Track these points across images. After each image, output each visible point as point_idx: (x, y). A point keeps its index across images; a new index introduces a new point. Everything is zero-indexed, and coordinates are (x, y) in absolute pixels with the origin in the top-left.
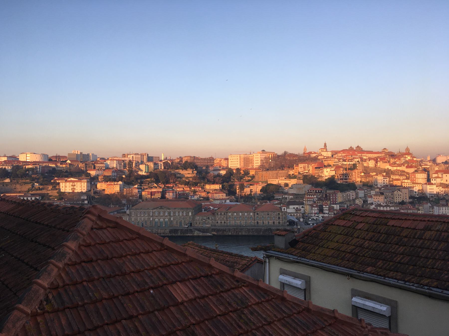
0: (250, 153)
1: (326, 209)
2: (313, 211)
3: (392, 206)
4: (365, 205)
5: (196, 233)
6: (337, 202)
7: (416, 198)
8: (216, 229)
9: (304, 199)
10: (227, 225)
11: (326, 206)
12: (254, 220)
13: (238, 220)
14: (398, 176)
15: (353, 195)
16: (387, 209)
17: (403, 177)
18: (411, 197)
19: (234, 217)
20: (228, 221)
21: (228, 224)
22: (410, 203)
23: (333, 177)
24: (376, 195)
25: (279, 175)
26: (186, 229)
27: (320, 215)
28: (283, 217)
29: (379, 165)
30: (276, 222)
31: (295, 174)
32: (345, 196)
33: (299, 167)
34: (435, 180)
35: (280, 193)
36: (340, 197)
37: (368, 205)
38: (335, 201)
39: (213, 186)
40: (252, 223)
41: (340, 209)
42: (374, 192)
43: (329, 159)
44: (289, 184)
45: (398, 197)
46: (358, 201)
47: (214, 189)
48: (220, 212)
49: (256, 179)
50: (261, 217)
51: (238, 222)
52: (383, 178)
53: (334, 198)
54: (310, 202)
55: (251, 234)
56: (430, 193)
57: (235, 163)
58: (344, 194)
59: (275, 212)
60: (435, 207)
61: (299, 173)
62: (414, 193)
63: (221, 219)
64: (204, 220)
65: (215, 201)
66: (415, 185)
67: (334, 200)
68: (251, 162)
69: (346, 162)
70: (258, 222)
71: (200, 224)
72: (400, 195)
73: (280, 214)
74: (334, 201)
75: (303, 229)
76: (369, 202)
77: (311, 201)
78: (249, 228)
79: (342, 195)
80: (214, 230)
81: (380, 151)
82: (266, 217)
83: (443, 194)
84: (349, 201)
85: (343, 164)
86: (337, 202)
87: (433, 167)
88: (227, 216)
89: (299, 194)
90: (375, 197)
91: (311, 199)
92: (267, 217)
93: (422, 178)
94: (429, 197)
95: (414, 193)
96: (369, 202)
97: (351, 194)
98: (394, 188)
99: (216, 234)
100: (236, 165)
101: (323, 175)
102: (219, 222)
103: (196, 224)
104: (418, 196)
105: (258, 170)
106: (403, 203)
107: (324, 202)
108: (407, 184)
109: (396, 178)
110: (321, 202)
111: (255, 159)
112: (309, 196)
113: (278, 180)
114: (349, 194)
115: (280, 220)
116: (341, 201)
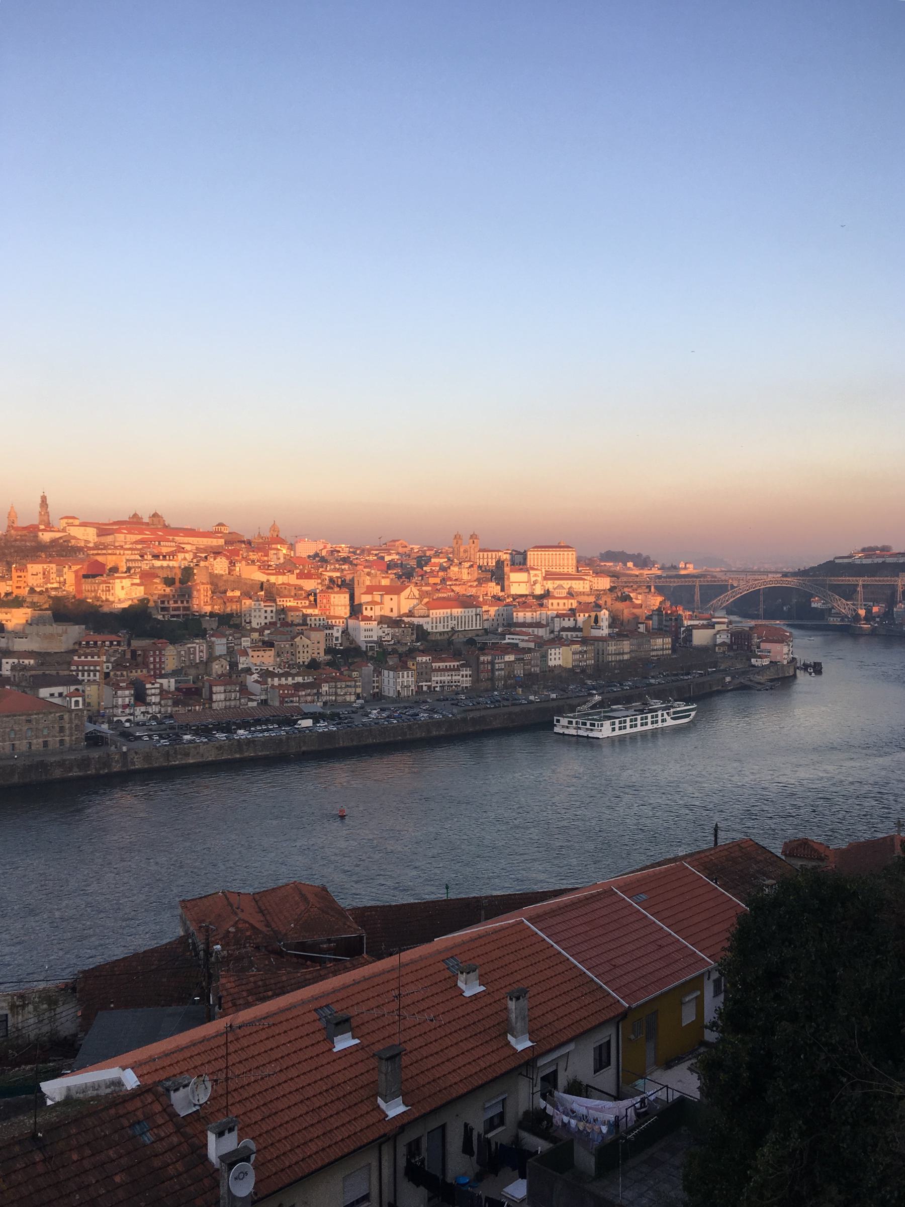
1: (153, 691)
2: (120, 701)
3: (298, 674)
4: (235, 675)
6: (163, 672)
7: (339, 651)
9: (73, 668)
11: (153, 684)
14: (292, 599)
16: (286, 682)
17: (303, 602)
18: (328, 651)
22: (330, 664)
23: (144, 602)
24: (255, 648)
27: (138, 708)
29: (238, 569)
30: (54, 742)
31: (16, 592)
32: (183, 653)
33: (30, 573)
36: (171, 657)
37: (242, 675)
38: (161, 669)
41: (176, 689)
42: (247, 641)
43: (110, 552)
45: (301, 652)
46: (217, 667)
50: (8, 730)
52: (265, 606)
53: (158, 660)
54: (92, 674)
56: (366, 639)
58: (180, 648)
59: (51, 713)
60: (386, 672)
61: (32, 591)
62: (334, 639)
66: (336, 622)
67: (158, 666)
69: (159, 560)
72: (305, 646)
73: (65, 717)
74: (157, 669)
75: (136, 753)
76: (241, 666)
77: (95, 671)
82: (21, 730)
83: (389, 641)
84: (196, 666)
85: (153, 567)
86: (163, 672)
89: (48, 654)
91: (95, 666)
92: (25, 728)
93: (343, 603)
94: (364, 649)
95: (334, 639)
96: (241, 666)
97: (198, 648)
101: (111, 598)
104: (341, 648)
106: (314, 665)
107: (131, 672)
108: (315, 620)
109: (289, 604)
110: (125, 673)
114: (192, 647)
116: (174, 668)
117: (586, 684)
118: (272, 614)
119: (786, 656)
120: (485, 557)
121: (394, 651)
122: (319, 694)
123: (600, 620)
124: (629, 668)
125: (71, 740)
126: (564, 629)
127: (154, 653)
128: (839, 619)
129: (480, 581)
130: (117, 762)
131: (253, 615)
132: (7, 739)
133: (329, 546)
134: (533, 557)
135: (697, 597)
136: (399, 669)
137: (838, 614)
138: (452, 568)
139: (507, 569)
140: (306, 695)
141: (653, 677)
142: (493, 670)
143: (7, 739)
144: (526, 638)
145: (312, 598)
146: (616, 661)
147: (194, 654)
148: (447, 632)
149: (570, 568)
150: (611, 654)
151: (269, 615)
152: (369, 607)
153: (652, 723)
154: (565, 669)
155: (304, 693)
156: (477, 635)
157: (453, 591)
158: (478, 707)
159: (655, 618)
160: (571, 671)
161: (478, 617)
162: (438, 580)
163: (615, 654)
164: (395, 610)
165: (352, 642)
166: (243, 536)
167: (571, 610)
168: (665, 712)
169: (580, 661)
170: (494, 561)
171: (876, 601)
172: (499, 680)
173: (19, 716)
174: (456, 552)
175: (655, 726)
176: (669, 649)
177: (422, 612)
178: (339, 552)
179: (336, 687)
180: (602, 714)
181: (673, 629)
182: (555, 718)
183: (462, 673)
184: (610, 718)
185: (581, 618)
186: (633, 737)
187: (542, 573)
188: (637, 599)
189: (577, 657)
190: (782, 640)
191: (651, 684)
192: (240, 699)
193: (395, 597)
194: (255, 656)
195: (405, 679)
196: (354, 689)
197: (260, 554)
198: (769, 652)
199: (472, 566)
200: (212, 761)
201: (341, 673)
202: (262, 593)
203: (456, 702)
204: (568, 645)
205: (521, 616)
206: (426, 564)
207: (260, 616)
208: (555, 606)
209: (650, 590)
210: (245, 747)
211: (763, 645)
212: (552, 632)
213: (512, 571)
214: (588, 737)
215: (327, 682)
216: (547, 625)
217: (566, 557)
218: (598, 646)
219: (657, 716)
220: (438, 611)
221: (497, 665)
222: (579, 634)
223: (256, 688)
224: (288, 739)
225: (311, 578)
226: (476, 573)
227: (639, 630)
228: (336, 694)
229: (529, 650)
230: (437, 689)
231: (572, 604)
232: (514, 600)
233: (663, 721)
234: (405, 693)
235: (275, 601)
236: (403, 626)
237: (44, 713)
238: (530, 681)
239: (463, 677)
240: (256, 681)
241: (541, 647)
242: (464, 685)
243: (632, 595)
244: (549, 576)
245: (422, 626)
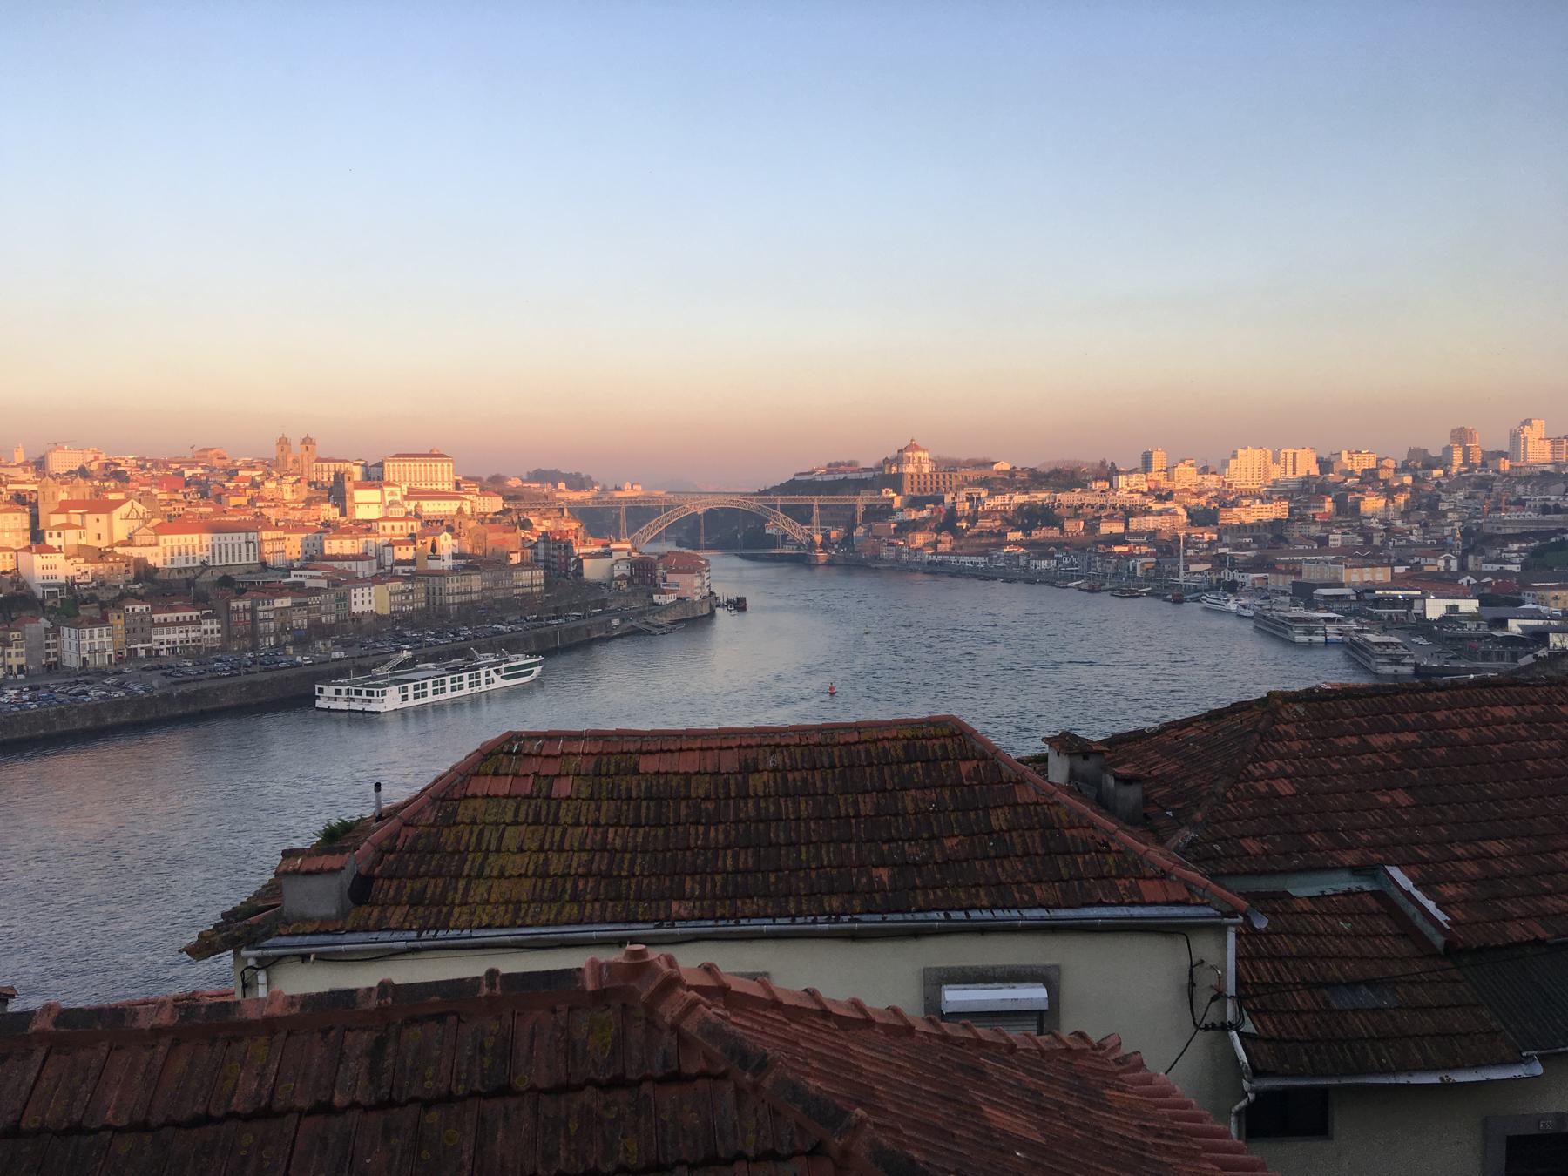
34: (59, 535)
56: (46, 581)
60: (66, 629)
83: (87, 583)
93: (12, 527)
94: (40, 596)
119: (698, 591)
124: (472, 612)
126: (401, 563)
150: (452, 594)
152: (55, 533)
161: (251, 546)
163: (458, 594)
164: (105, 536)
167: (412, 536)
169: (404, 605)
177: (147, 540)
182: (317, 686)
190: (694, 568)
193: (103, 517)
198: (678, 586)
205: (333, 546)
208: (389, 531)
211: (670, 578)
216: (378, 556)
230: (163, 653)
231: (412, 527)
236: (111, 559)
242: (209, 645)
244: (413, 494)
245: (145, 559)
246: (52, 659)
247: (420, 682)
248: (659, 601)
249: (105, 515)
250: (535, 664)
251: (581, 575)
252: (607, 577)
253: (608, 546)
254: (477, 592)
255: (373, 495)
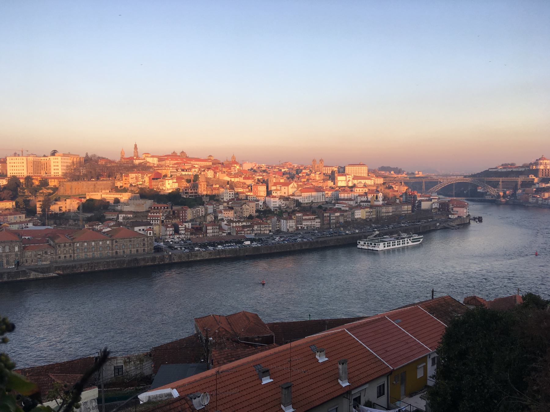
0: (22, 151)
1: (182, 229)
2: (168, 233)
3: (244, 221)
5: (33, 275)
6: (186, 220)
7: (262, 211)
8: (61, 266)
9: (149, 218)
10: (73, 259)
11: (182, 225)
12: (112, 250)
13: (90, 252)
15: (203, 211)
16: (239, 225)
17: (246, 189)
18: (257, 211)
19: (83, 248)
20: (75, 255)
21: (76, 258)
22: (258, 217)
23: (178, 190)
24: (225, 210)
25: (98, 187)
26: (15, 272)
27: (176, 236)
28: (149, 243)
29: (218, 175)
30: (141, 250)
31: (125, 186)
33: (130, 178)
34: (276, 193)
35: (111, 211)
36: (190, 214)
39: (3, 203)
40: (109, 253)
41: (192, 228)
43: (163, 168)
44: (120, 199)
46: (209, 218)
47: (4, 208)
48: (64, 243)
49: (61, 192)
50: (122, 245)
51: (90, 255)
52: (229, 192)
53: (184, 215)
54: (156, 221)
55: (111, 267)
57: (18, 168)
59: (139, 238)
61: (131, 185)
62: (260, 206)
63: (65, 252)
64: (39, 256)
65: (11, 226)
67: (184, 217)
68: (43, 167)
69: (184, 172)
70: (116, 252)
71: (32, 262)
73: (145, 239)
75: (175, 255)
76: (219, 218)
77: (157, 220)
78: (108, 261)
79: (191, 212)
80: (58, 268)
81: (206, 158)
83: (284, 207)
84: (200, 218)
85: (182, 175)
86: (186, 220)
87: (272, 179)
88: (74, 248)
89: (138, 212)
90: (225, 212)
91: (158, 218)
93: (263, 190)
94: (273, 210)
95: (260, 206)
96: (219, 218)
97: (201, 210)
98: (241, 201)
99: (62, 273)
100: (20, 172)
101: (164, 188)
102: (62, 256)
103: (27, 262)
105: (63, 180)
106: (251, 217)
107: (173, 220)
109: (240, 191)
110: (170, 221)
111: (52, 164)
112: (156, 214)
113: (101, 193)
115: (145, 248)
117: (372, 226)
118: (232, 195)
119: (465, 214)
120: (327, 169)
121: (286, 211)
122: (253, 230)
123: (378, 197)
125: (148, 250)
126: (362, 202)
127: (182, 212)
128: (490, 197)
129: (324, 180)
130: (167, 259)
131: (224, 195)
132: (121, 248)
133: (257, 165)
134: (348, 169)
135: (424, 187)
136: (288, 219)
137: (490, 195)
138: (312, 174)
139: (336, 175)
140: (247, 231)
141: (403, 223)
142: (330, 220)
143: (121, 248)
144: (345, 205)
145: (250, 188)
146: (386, 216)
147: (199, 212)
148: (309, 203)
149: (365, 174)
150: (384, 213)
151: (231, 195)
152: (275, 192)
153: (402, 244)
154: (363, 219)
155: (246, 230)
156: (323, 204)
157: (312, 184)
158: (323, 236)
159: (404, 196)
160: (366, 220)
162: (305, 180)
163: (385, 213)
164: (286, 193)
165: (268, 207)
166: (220, 161)
167: (365, 193)
168: (408, 239)
169: (369, 216)
170: (330, 171)
171: (508, 189)
172: (333, 224)
173: (126, 239)
174: (313, 167)
175: (404, 245)
176: (410, 210)
177: (298, 194)
178: (262, 167)
179: (260, 227)
180: (379, 240)
181: (412, 201)
183: (316, 221)
184: (383, 241)
185: (370, 196)
186: (393, 250)
187: (352, 177)
188: (396, 188)
189: (368, 214)
190: (463, 206)
191: (402, 227)
192: (219, 232)
194: (225, 213)
195: (291, 224)
196: (268, 228)
197: (227, 169)
198: (458, 212)
199: (320, 174)
200: (207, 259)
201: (263, 221)
202: (228, 186)
203: (313, 234)
204: (364, 209)
205: (342, 196)
206: (300, 173)
207: (227, 196)
208: (358, 191)
209: (402, 184)
210: (221, 253)
211: (454, 209)
212: (357, 203)
213: (338, 176)
214: (373, 250)
215: (257, 225)
216: (354, 200)
217: (363, 169)
218: (378, 209)
219: (405, 241)
220: (305, 193)
221: (332, 218)
222: (369, 204)
223: (225, 227)
224: (240, 249)
225: (249, 179)
226: (322, 177)
227: (397, 202)
228: (261, 230)
229: (346, 211)
230: (305, 228)
232: (339, 188)
233: (407, 243)
234: (290, 230)
235: (234, 189)
237: (137, 238)
238: (347, 224)
239: (316, 223)
240: (226, 225)
241: (351, 209)
242: (317, 226)
243: (393, 186)
244: (355, 178)
245: (298, 200)
246: (278, 229)
247: (389, 242)
248: (451, 217)
249: (287, 187)
250: (421, 238)
251: (421, 207)
252: (430, 208)
253: (429, 197)
254: (391, 212)
255: (343, 178)
